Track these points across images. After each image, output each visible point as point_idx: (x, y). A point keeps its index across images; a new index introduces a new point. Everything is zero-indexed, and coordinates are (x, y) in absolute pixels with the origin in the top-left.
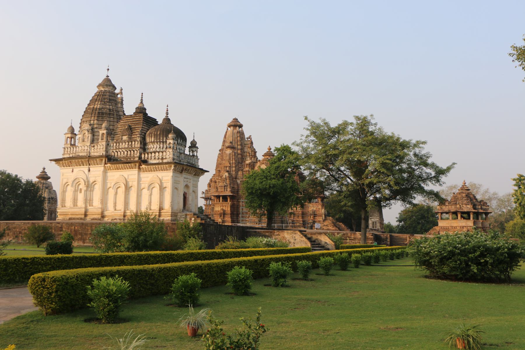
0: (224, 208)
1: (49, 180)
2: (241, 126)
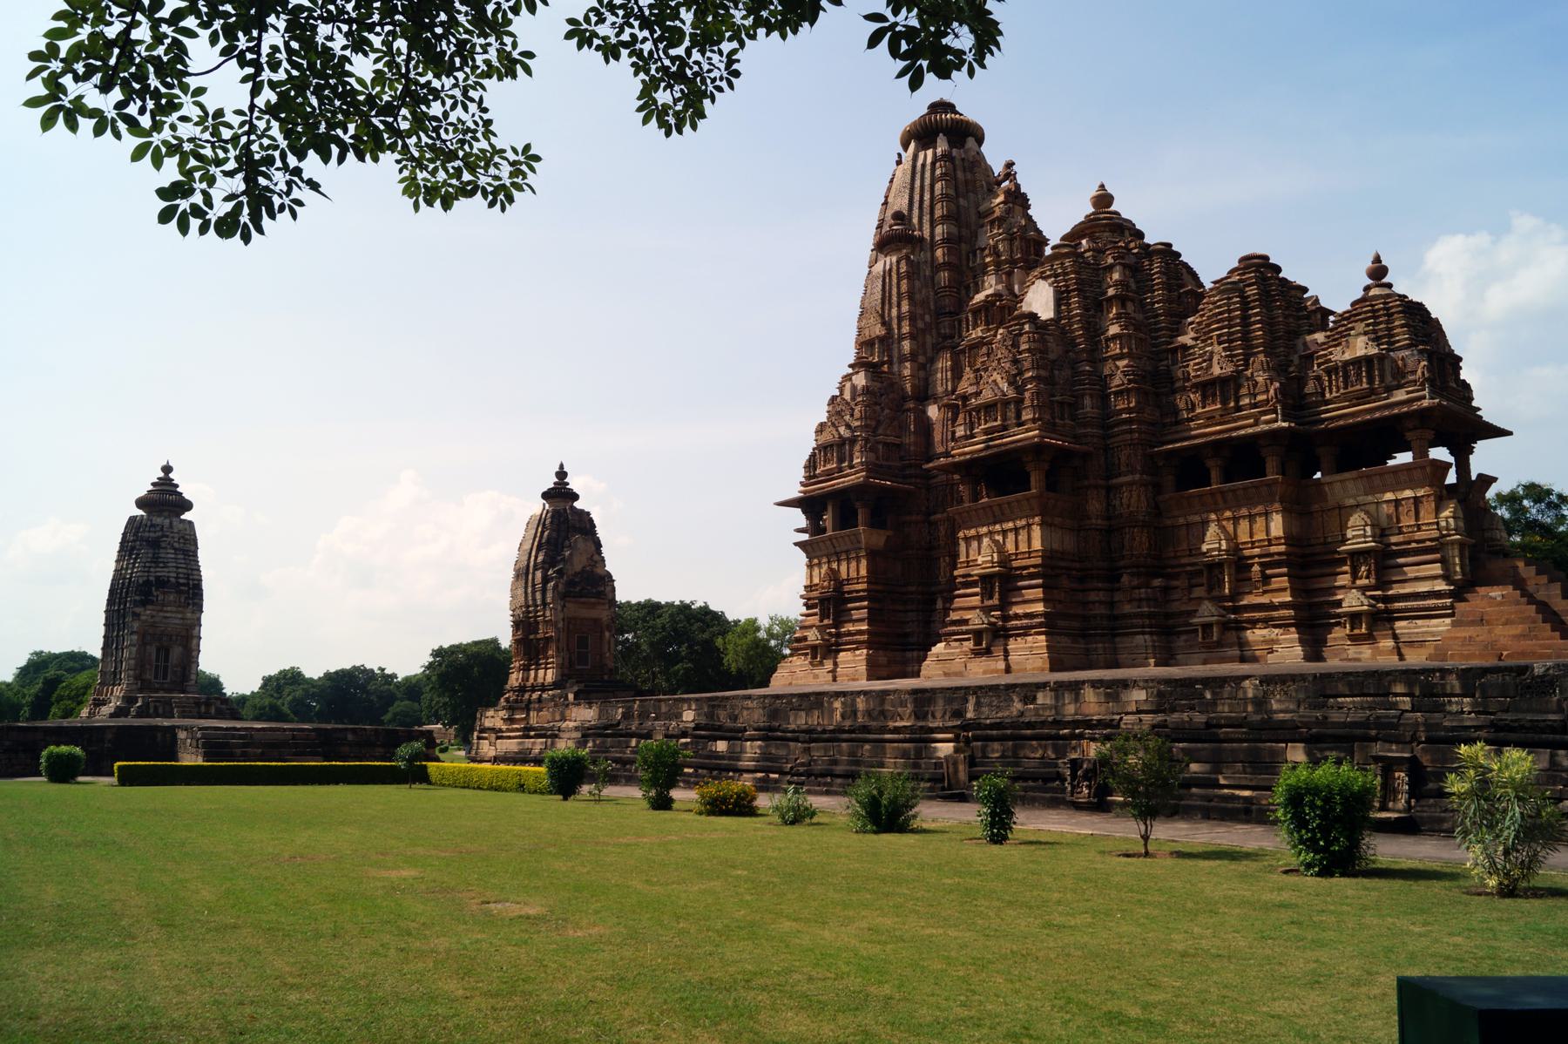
1: (186, 516)
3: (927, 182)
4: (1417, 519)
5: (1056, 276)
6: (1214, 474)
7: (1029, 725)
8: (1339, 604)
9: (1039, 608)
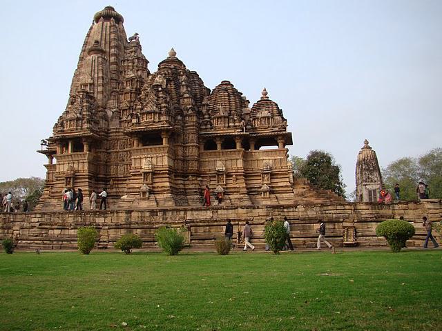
0: (76, 166)
2: (119, 19)
3: (108, 33)
5: (165, 74)
6: (219, 147)
7: (216, 221)
9: (168, 184)
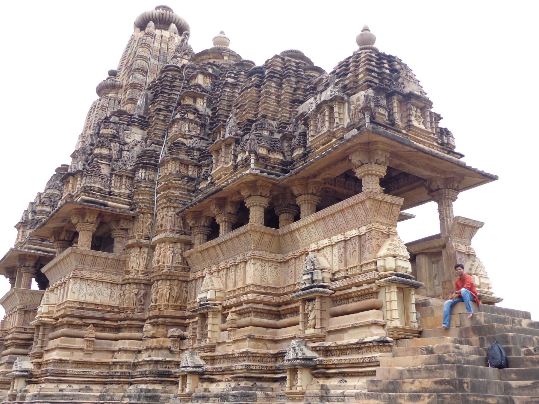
4: (360, 261)
8: (280, 355)
